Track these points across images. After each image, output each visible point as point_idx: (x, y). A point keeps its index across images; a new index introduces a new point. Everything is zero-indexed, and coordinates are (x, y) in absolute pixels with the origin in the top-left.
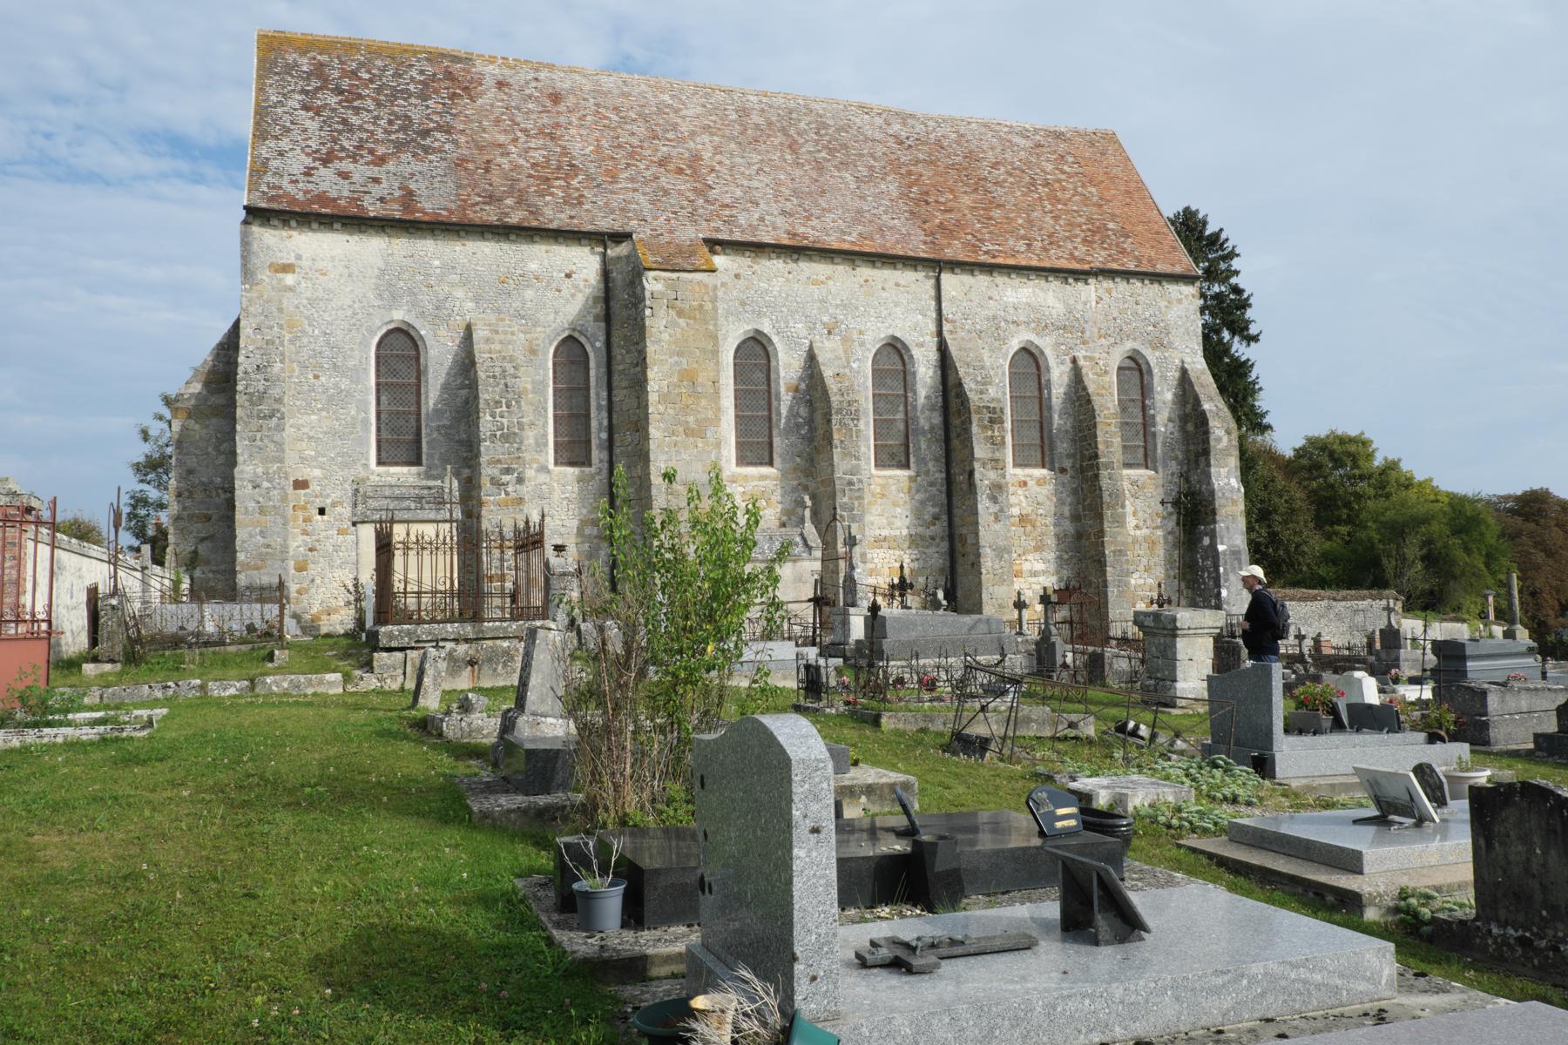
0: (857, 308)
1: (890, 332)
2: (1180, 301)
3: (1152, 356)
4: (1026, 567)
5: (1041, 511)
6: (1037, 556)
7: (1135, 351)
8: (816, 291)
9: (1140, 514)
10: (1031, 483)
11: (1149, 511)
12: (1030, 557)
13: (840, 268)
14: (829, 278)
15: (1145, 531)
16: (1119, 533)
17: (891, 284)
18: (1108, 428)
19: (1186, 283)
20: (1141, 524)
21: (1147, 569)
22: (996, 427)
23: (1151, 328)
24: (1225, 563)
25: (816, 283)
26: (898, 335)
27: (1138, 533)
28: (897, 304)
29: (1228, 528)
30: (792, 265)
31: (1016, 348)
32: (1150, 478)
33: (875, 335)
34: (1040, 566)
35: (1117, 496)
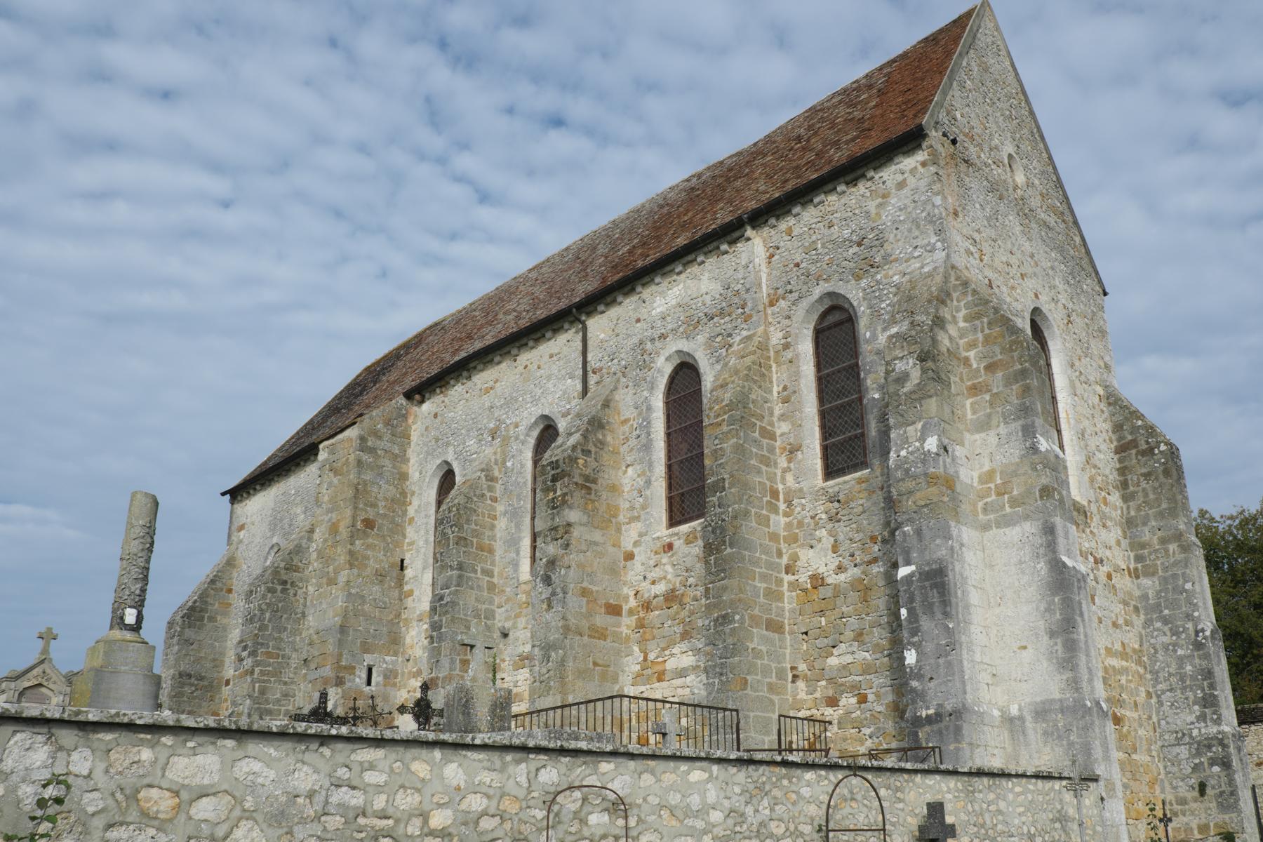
0: (517, 400)
1: (540, 412)
2: (901, 185)
3: (854, 293)
4: (671, 664)
5: (691, 580)
6: (684, 646)
7: (830, 295)
8: (487, 400)
9: (845, 547)
10: (678, 544)
11: (857, 537)
12: (676, 650)
13: (503, 365)
14: (496, 381)
15: (854, 572)
16: (725, 588)
17: (546, 358)
18: (718, 431)
19: (909, 152)
20: (846, 562)
21: (859, 636)
22: (558, 484)
23: (855, 249)
24: (911, 600)
25: (488, 390)
26: (546, 412)
27: (842, 577)
28: (549, 378)
29: (919, 532)
30: (469, 384)
31: (668, 369)
32: (860, 481)
33: (526, 418)
34: (688, 660)
35: (723, 530)
